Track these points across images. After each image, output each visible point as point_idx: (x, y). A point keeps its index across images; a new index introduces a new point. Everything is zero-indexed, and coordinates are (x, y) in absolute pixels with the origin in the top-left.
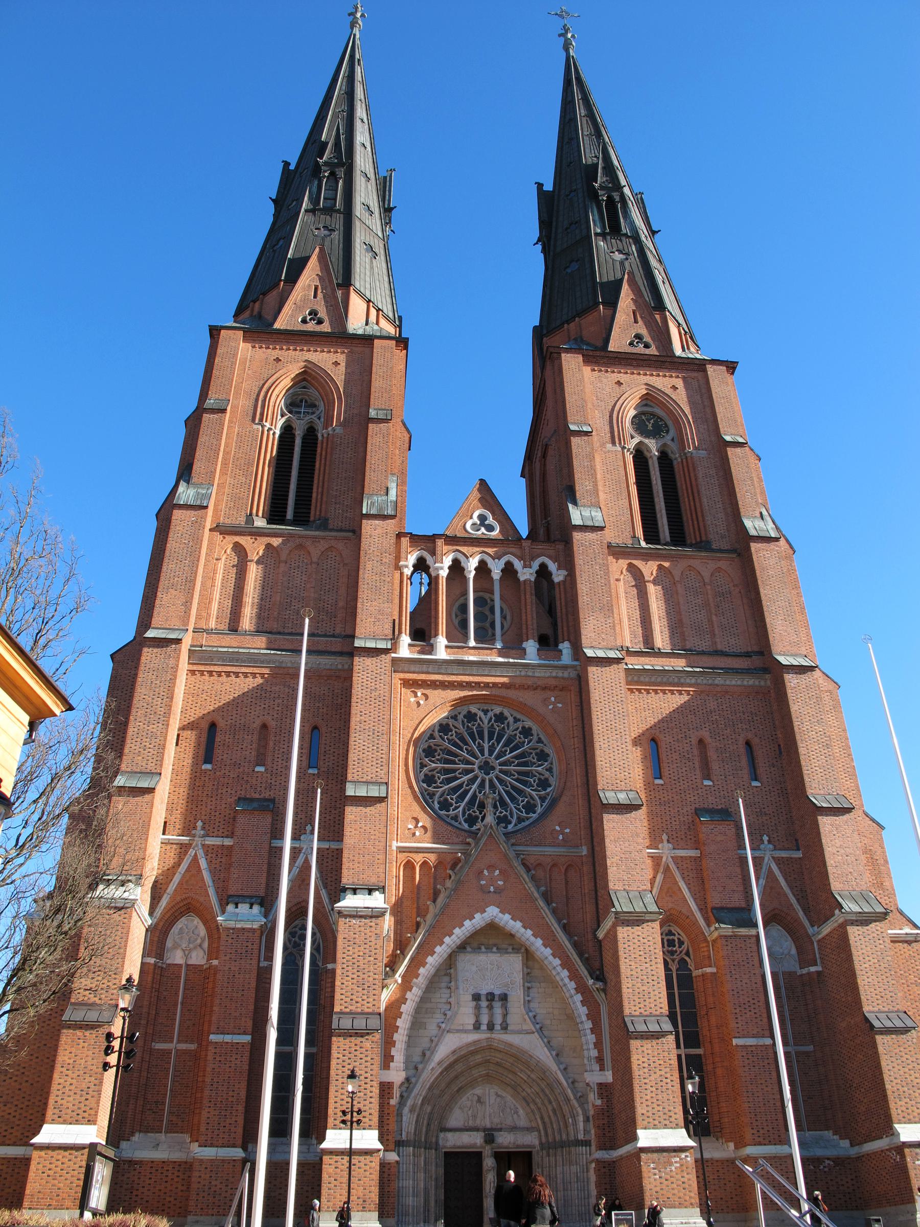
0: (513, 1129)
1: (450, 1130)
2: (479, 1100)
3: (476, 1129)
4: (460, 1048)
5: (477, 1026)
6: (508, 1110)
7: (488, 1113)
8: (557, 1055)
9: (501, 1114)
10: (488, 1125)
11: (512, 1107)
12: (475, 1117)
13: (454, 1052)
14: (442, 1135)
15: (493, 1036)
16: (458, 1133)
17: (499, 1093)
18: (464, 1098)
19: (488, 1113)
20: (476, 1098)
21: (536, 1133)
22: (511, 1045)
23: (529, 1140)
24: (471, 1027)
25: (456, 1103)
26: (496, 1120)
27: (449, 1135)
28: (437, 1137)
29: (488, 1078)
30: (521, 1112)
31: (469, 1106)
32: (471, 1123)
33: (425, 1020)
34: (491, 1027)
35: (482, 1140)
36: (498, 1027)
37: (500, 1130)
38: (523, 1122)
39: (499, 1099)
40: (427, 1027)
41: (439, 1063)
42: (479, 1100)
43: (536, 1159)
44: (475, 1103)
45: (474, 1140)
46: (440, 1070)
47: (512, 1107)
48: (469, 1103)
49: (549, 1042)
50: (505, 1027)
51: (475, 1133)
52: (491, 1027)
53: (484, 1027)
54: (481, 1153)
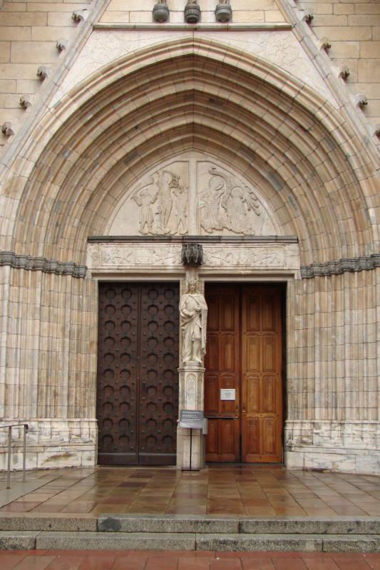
0: (244, 240)
1: (111, 240)
2: (175, 183)
3: (168, 239)
4: (122, 63)
5: (161, 16)
6: (238, 201)
7: (192, 209)
8: (345, 76)
9: (222, 210)
10: (194, 232)
11: (246, 196)
12: (164, 214)
13: (108, 70)
14: (92, 248)
15: (198, 35)
16: (126, 245)
17: (219, 170)
18: (144, 180)
19: (192, 209)
20: (168, 178)
21: (294, 246)
22: (239, 55)
23: (281, 260)
24: (147, 19)
25: (127, 188)
26: (210, 222)
27: (109, 249)
28: (83, 252)
29: (196, 138)
30: (265, 205)
31: (153, 193)
32: (156, 229)
33: (45, 8)
34: (192, 17)
35: (178, 259)
36: (208, 19)
37: (218, 240)
38: (267, 228)
39: (217, 180)
40: (52, 20)
41: (74, 95)
42: (175, 183)
43: (294, 296)
44: (166, 187)
45: (167, 259)
46: (75, 107)
47: (246, 196)
48: (153, 190)
49: (327, 48)
50: (223, 17)
51: (163, 245)
52: (192, 17)
53: (177, 19)
54: (177, 284)
